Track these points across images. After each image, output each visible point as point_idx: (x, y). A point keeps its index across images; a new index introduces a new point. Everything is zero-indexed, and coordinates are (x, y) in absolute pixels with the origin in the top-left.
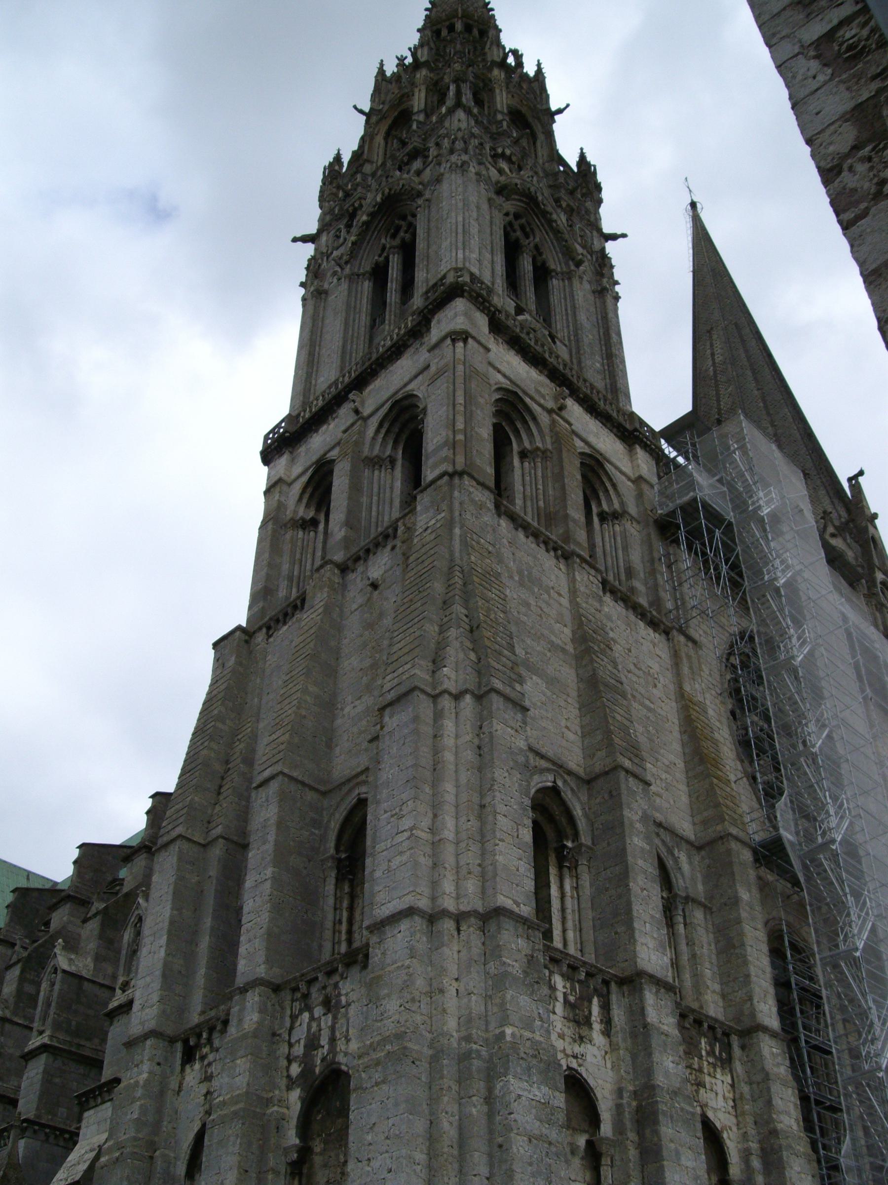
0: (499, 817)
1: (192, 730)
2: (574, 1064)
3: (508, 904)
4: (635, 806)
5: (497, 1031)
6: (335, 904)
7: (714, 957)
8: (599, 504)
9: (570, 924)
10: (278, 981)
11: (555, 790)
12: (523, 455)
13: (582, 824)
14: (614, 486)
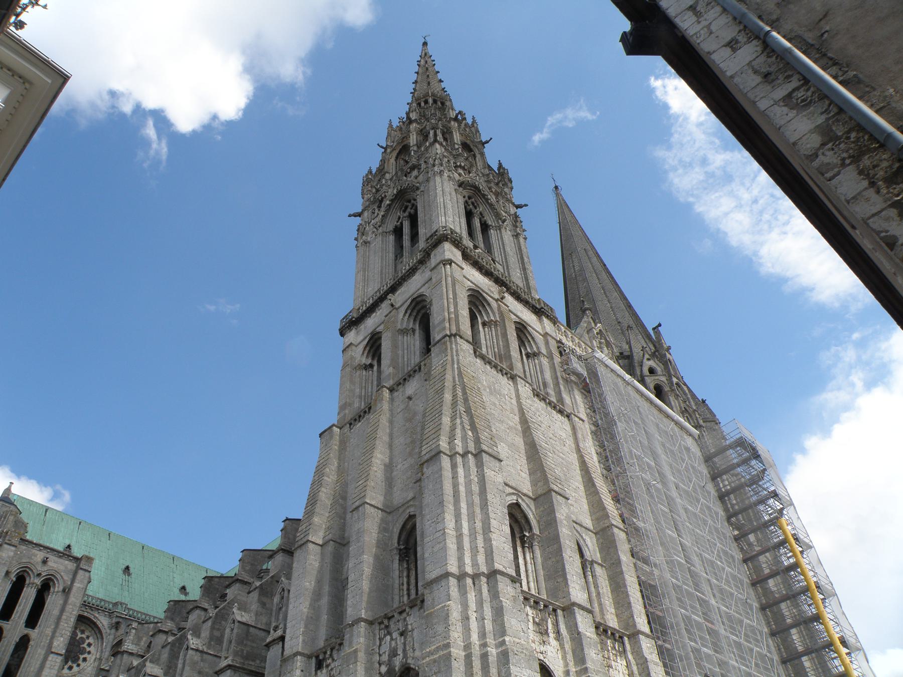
2: (542, 658)
3: (501, 568)
4: (562, 511)
5: (501, 640)
8: (526, 349)
9: (531, 579)
10: (370, 619)
12: (484, 324)
14: (533, 338)
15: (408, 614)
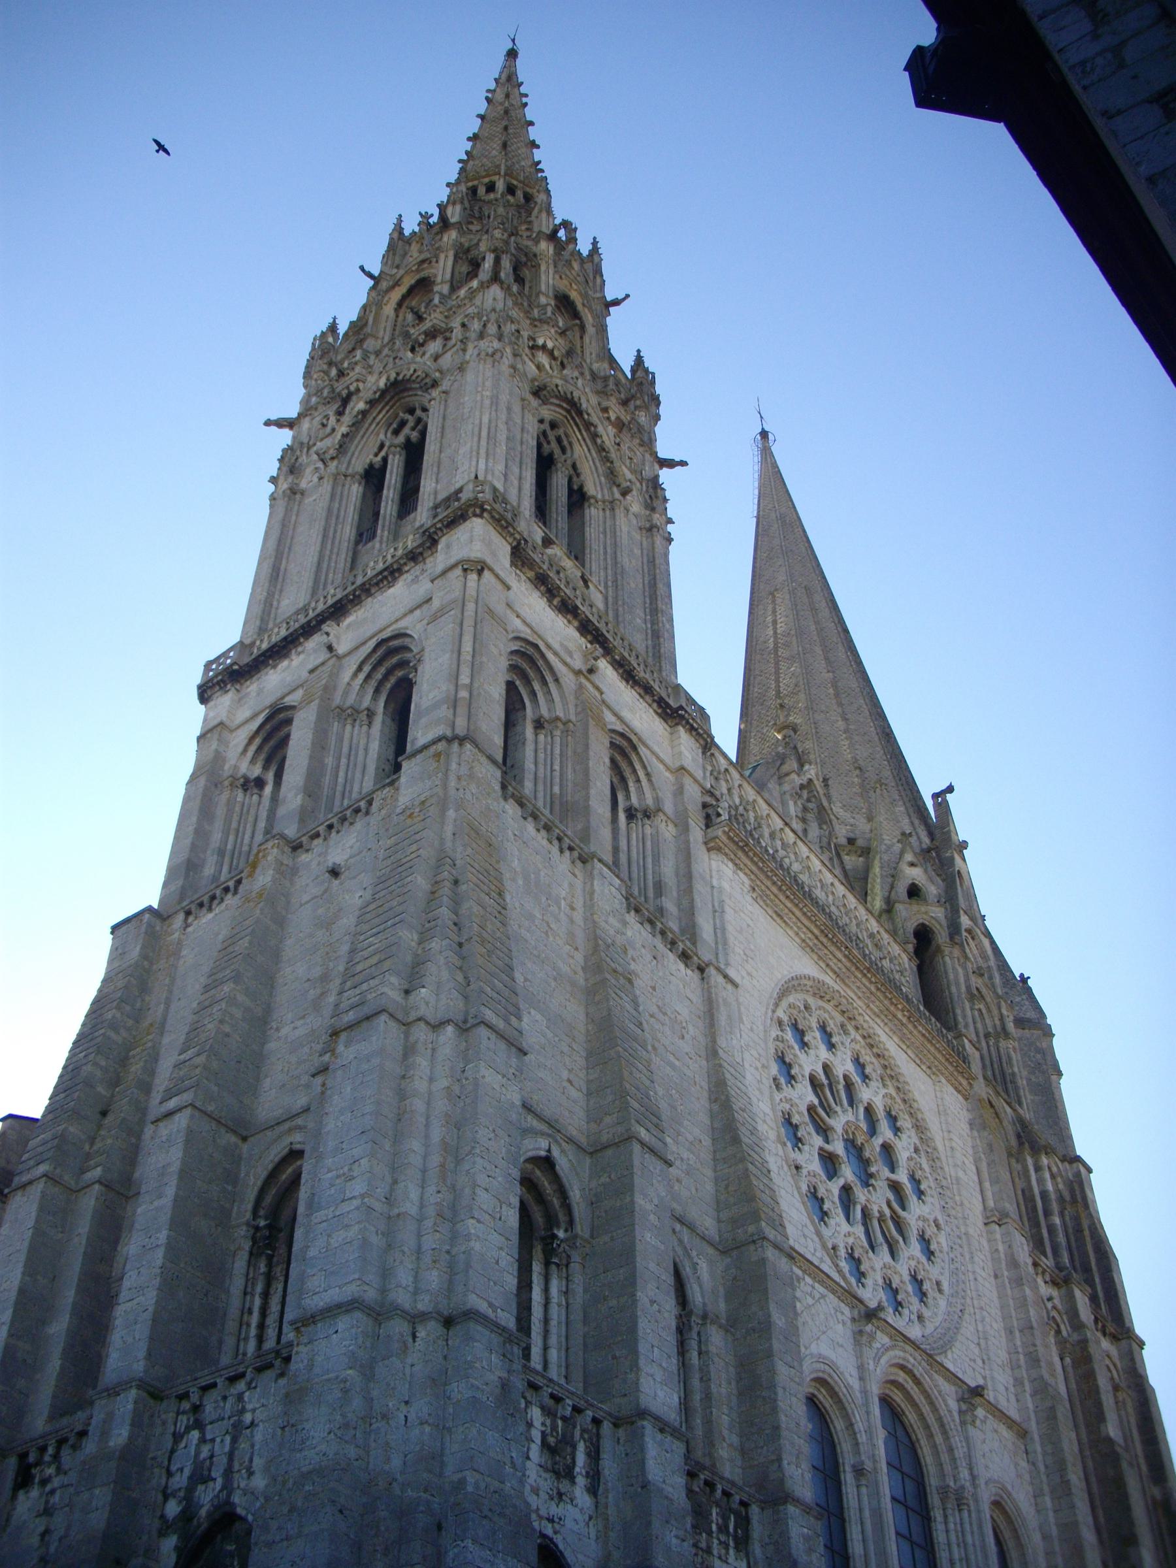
0: (478, 1191)
1: (73, 1037)
3: (483, 1307)
6: (246, 1287)
7: (734, 1399)
8: (628, 797)
9: (553, 1340)
11: (547, 1163)
12: (539, 725)
13: (580, 1209)
15: (249, 1384)
